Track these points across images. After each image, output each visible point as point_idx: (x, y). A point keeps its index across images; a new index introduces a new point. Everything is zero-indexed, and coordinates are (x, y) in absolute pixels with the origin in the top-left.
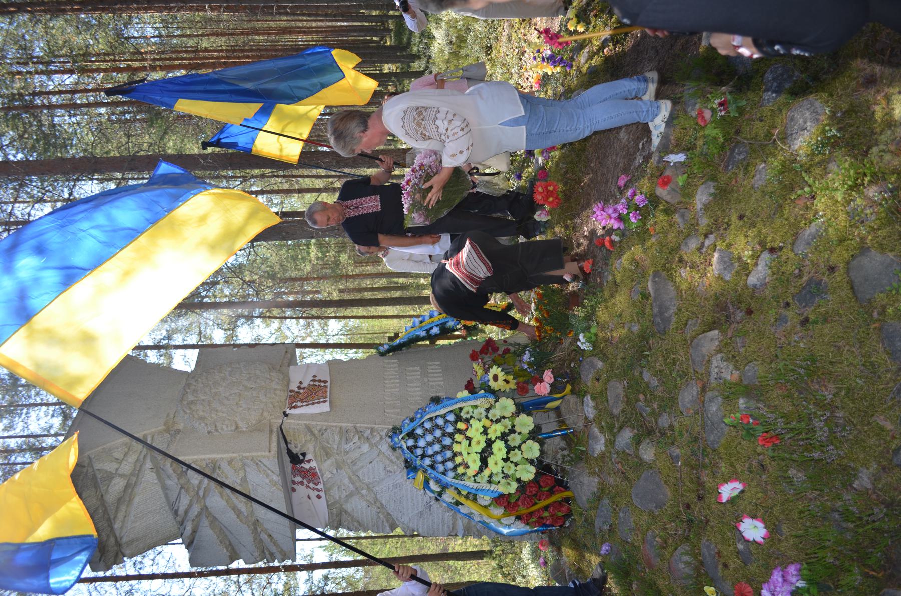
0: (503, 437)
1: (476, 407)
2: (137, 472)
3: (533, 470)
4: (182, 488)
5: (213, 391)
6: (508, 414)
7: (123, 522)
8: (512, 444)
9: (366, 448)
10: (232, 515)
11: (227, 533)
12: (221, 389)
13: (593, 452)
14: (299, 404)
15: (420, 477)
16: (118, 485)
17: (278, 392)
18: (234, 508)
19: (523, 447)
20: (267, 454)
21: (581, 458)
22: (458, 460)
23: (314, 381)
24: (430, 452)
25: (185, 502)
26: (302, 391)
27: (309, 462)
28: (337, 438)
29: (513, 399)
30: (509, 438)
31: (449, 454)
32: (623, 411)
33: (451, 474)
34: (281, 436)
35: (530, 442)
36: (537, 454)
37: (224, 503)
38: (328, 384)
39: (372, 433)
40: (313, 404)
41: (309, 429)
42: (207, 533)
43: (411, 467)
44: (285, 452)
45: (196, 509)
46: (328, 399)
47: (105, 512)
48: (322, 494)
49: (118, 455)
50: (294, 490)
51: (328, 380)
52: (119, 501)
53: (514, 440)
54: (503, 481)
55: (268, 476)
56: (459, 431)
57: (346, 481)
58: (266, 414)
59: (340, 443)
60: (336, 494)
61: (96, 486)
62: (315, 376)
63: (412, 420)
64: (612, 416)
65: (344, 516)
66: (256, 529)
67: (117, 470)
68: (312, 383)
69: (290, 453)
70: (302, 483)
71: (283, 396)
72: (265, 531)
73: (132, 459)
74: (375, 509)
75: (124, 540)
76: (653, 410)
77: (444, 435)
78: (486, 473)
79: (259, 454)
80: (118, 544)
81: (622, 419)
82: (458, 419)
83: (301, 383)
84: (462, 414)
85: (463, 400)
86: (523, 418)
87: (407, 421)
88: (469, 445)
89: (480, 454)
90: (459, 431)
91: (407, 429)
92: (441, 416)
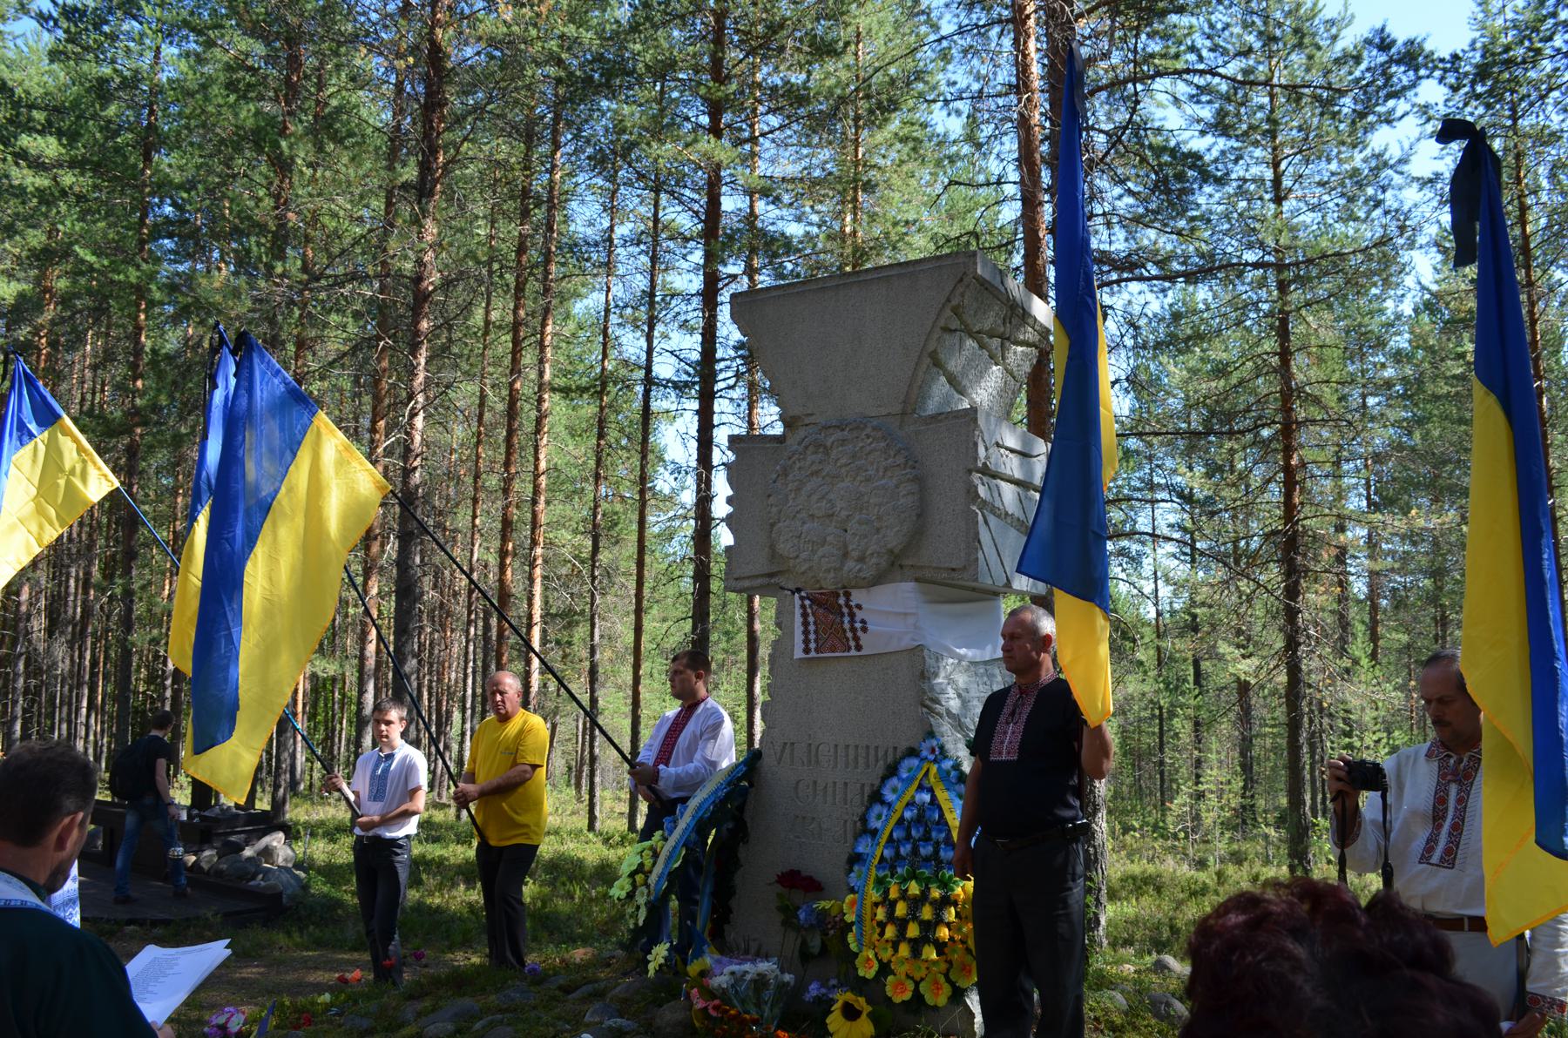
23: (853, 630)
38: (853, 652)
46: (813, 654)
51: (862, 653)
71: (829, 584)
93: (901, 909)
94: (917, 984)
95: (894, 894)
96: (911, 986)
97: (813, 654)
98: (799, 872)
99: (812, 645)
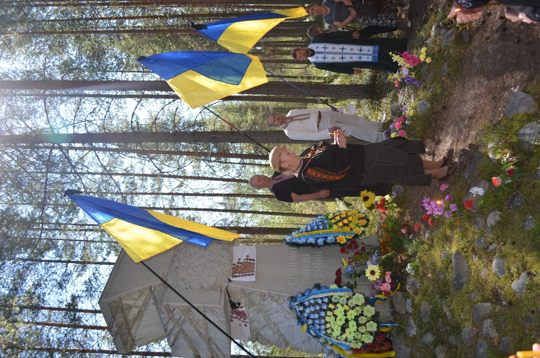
0: (356, 319)
1: (341, 297)
2: (146, 304)
3: (372, 338)
4: (170, 319)
5: (189, 261)
6: (360, 304)
7: (136, 330)
8: (360, 322)
9: (275, 304)
10: (197, 335)
11: (193, 343)
12: (194, 260)
13: (409, 333)
14: (238, 274)
15: (305, 327)
16: (134, 311)
17: (226, 265)
18: (198, 331)
19: (367, 324)
20: (218, 306)
21: (402, 331)
22: (328, 326)
23: (247, 259)
24: (312, 317)
25: (171, 326)
26: (240, 265)
27: (241, 307)
28: (258, 298)
29: (363, 294)
30: (359, 319)
31: (323, 321)
32: (429, 322)
33: (323, 332)
34: (226, 293)
35: (371, 322)
36: (375, 329)
37: (192, 328)
39: (279, 298)
40: (246, 275)
41: (243, 291)
42: (182, 341)
43: (301, 321)
44: (228, 301)
45: (177, 330)
47: (127, 324)
48: (248, 324)
49: (136, 296)
50: (232, 321)
52: (135, 319)
53: (362, 320)
54: (354, 341)
55: (218, 318)
56: (330, 310)
57: (262, 320)
58: (218, 279)
59: (260, 300)
60: (256, 325)
61: (123, 312)
62: (248, 256)
63: (303, 295)
64: (422, 322)
65: (259, 336)
66: (209, 342)
67: (134, 304)
68: (246, 261)
69: (231, 302)
70: (237, 318)
71: (229, 267)
72: (215, 344)
73: (143, 298)
74: (277, 336)
75: (137, 338)
76: (447, 330)
77: (321, 310)
78: (344, 336)
79: (214, 305)
80: (133, 340)
81: (428, 327)
82: (330, 301)
83: (239, 259)
84: (332, 299)
85: (334, 291)
86: (369, 307)
87: (300, 295)
88: (335, 320)
89: (342, 327)
90: (330, 310)
91: (300, 299)
92: (320, 298)
93: (338, 218)
97: (254, 273)
98: (336, 280)
99: (251, 273)
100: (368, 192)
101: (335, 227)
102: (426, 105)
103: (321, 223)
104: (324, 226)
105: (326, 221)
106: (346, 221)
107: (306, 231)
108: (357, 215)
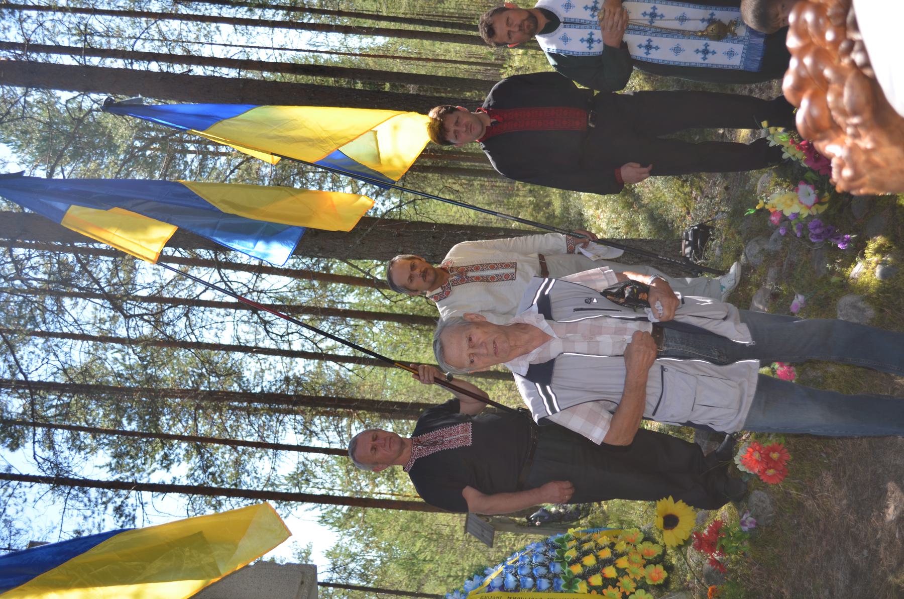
93: (590, 561)
94: (649, 562)
95: (577, 569)
96: (651, 568)
100: (675, 502)
101: (582, 587)
102: (863, 310)
103: (542, 571)
104: (551, 584)
105: (558, 568)
106: (610, 572)
107: (502, 588)
108: (640, 547)
